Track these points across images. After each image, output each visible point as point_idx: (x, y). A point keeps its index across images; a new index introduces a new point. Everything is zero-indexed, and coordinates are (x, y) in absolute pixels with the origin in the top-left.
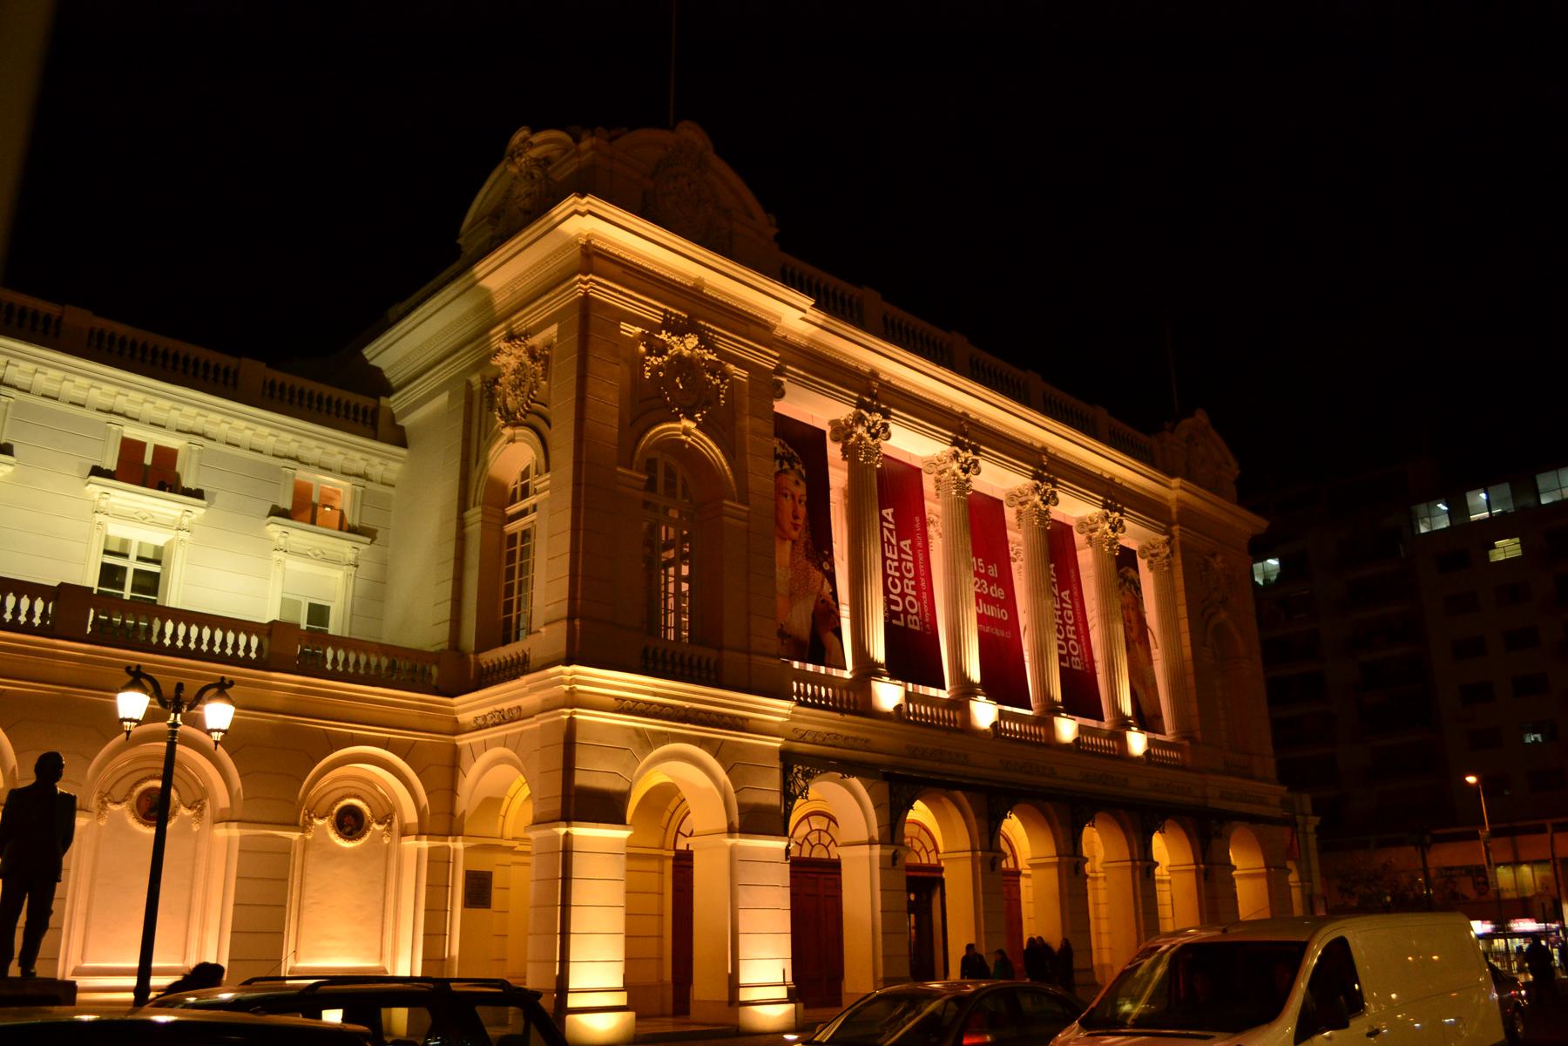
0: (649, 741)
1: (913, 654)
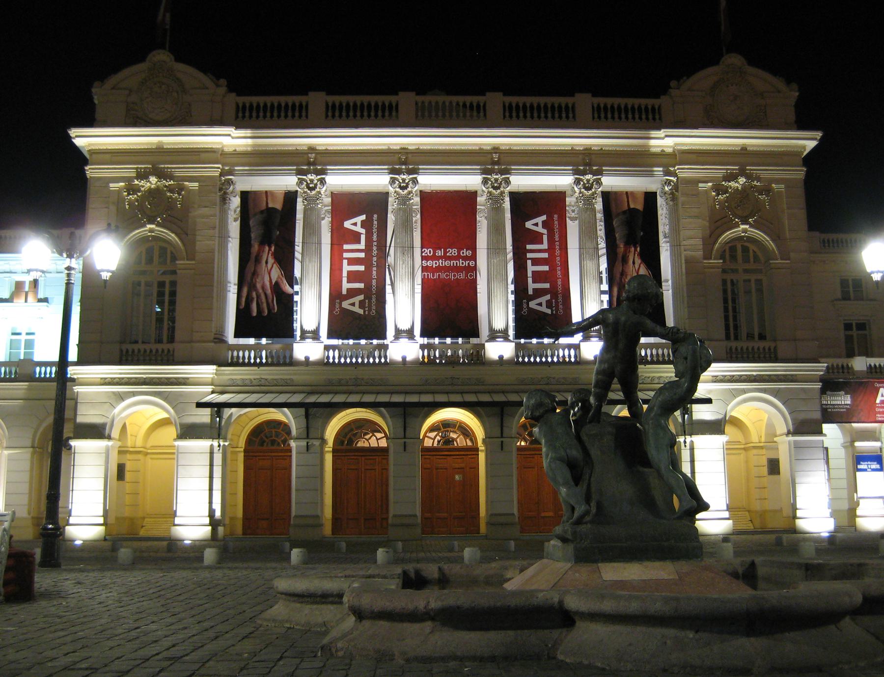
0: (121, 397)
1: (358, 319)
